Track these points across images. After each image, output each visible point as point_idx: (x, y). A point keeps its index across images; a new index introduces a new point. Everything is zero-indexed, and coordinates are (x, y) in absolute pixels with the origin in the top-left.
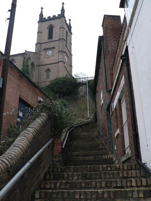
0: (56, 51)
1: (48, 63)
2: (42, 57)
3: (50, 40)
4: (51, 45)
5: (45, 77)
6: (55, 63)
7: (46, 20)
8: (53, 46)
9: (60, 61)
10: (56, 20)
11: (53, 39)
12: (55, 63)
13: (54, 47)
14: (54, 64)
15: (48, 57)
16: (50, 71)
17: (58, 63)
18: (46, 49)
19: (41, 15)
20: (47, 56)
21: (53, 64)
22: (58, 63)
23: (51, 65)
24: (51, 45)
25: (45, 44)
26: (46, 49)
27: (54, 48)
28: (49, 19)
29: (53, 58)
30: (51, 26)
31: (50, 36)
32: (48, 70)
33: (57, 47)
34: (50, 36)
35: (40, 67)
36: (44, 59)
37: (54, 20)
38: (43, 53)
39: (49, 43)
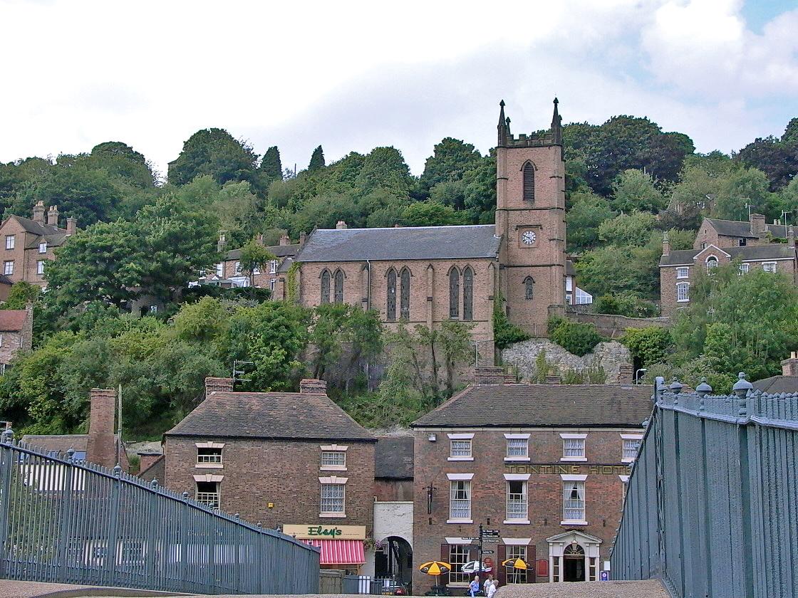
0: (544, 235)
2: (514, 244)
3: (528, 205)
4: (533, 218)
6: (543, 266)
11: (538, 204)
12: (543, 266)
13: (540, 225)
18: (518, 227)
19: (504, 125)
20: (523, 245)
21: (540, 266)
24: (533, 218)
25: (518, 212)
29: (537, 252)
31: (528, 195)
33: (546, 226)
34: (528, 195)
37: (537, 149)
38: (513, 235)
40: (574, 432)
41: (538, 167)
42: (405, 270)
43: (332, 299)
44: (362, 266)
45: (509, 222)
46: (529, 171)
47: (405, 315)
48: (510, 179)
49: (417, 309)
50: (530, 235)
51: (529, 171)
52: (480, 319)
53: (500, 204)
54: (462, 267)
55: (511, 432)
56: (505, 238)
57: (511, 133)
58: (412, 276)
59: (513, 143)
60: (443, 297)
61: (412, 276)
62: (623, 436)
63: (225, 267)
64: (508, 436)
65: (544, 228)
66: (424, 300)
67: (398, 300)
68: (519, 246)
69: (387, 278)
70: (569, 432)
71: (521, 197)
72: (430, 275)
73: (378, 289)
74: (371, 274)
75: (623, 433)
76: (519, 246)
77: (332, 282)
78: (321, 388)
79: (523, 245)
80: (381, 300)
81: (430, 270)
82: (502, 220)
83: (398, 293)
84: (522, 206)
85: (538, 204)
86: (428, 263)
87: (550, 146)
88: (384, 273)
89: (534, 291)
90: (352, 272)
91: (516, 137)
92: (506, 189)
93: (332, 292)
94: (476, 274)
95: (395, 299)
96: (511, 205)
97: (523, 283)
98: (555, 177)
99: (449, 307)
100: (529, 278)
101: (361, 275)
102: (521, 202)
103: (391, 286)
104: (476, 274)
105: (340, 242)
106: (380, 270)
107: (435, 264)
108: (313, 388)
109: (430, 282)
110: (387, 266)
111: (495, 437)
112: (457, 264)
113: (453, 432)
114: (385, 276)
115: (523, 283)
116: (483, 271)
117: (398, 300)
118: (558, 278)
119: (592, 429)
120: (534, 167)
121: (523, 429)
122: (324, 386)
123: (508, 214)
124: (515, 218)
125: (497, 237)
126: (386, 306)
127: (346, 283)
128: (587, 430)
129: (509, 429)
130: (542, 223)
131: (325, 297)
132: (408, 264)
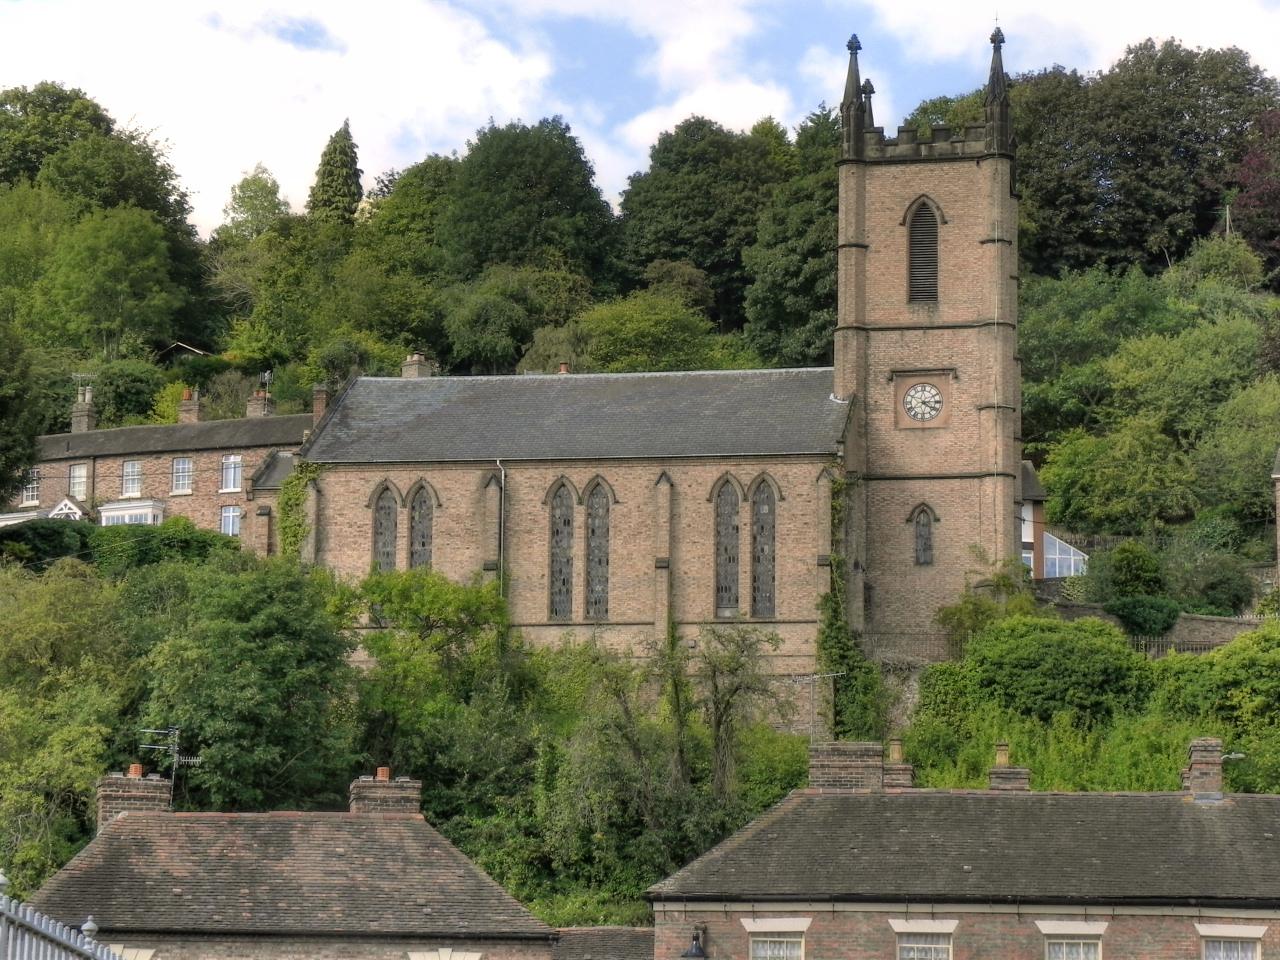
0: (962, 396)
1: (923, 465)
2: (882, 420)
3: (920, 316)
4: (934, 350)
5: (909, 555)
7: (890, 151)
8: (946, 363)
9: (993, 469)
10: (957, 165)
11: (946, 313)
14: (956, 483)
15: (919, 425)
16: (937, 520)
17: (981, 476)
18: (898, 374)
20: (906, 422)
22: (981, 476)
23: (937, 485)
24: (934, 350)
25: (895, 335)
26: (898, 374)
27: (948, 372)
28: (903, 149)
29: (945, 439)
30: (924, 204)
31: (922, 288)
32: (922, 514)
33: (968, 372)
34: (922, 288)
35: (873, 484)
36: (899, 437)
37: (946, 167)
38: (881, 394)
39: (920, 333)
40: (1072, 917)
41: (949, 213)
42: (595, 487)
43: (401, 562)
44: (484, 477)
45: (871, 360)
46: (922, 223)
47: (597, 606)
48: (873, 247)
49: (630, 590)
50: (921, 396)
51: (922, 223)
52: (794, 617)
53: (846, 312)
54: (746, 480)
55: (907, 916)
56: (858, 404)
57: (876, 125)
58: (617, 502)
59: (882, 151)
60: (697, 560)
61: (617, 502)
62: (1204, 929)
63: (93, 478)
64: (899, 925)
65: (964, 377)
66: (645, 565)
67: (579, 565)
68: (896, 423)
69: (548, 509)
70: (1060, 917)
71: (902, 292)
72: (663, 500)
73: (527, 537)
74: (506, 497)
75: (1201, 919)
76: (896, 423)
77: (403, 517)
78: (407, 800)
79: (906, 422)
80: (532, 560)
81: (664, 487)
82: (852, 355)
83: (578, 549)
84: (906, 318)
85: (946, 313)
86: (657, 470)
87: (979, 159)
88: (542, 494)
89: (936, 541)
90: (457, 489)
91: (891, 133)
92: (861, 272)
93: (402, 544)
94: (783, 499)
95: (569, 561)
96: (874, 316)
97: (909, 521)
98: (993, 241)
99: (712, 583)
100: (924, 508)
101: (480, 500)
102: (903, 306)
103: (559, 530)
104: (783, 499)
105: (425, 411)
106: (530, 486)
107: (676, 472)
108: (384, 801)
109: (663, 518)
110: (550, 475)
111: (864, 928)
112: (733, 470)
113: (755, 915)
114: (544, 503)
115: (909, 521)
116: (804, 489)
117: (579, 565)
118: (1000, 508)
119: (1119, 911)
120: (937, 214)
121: (939, 908)
122: (415, 795)
123: (868, 338)
124: (886, 351)
125: (837, 399)
126: (546, 581)
127: (439, 522)
128: (1108, 911)
129: (901, 908)
130: (957, 362)
131: (382, 558)
132: (601, 470)
